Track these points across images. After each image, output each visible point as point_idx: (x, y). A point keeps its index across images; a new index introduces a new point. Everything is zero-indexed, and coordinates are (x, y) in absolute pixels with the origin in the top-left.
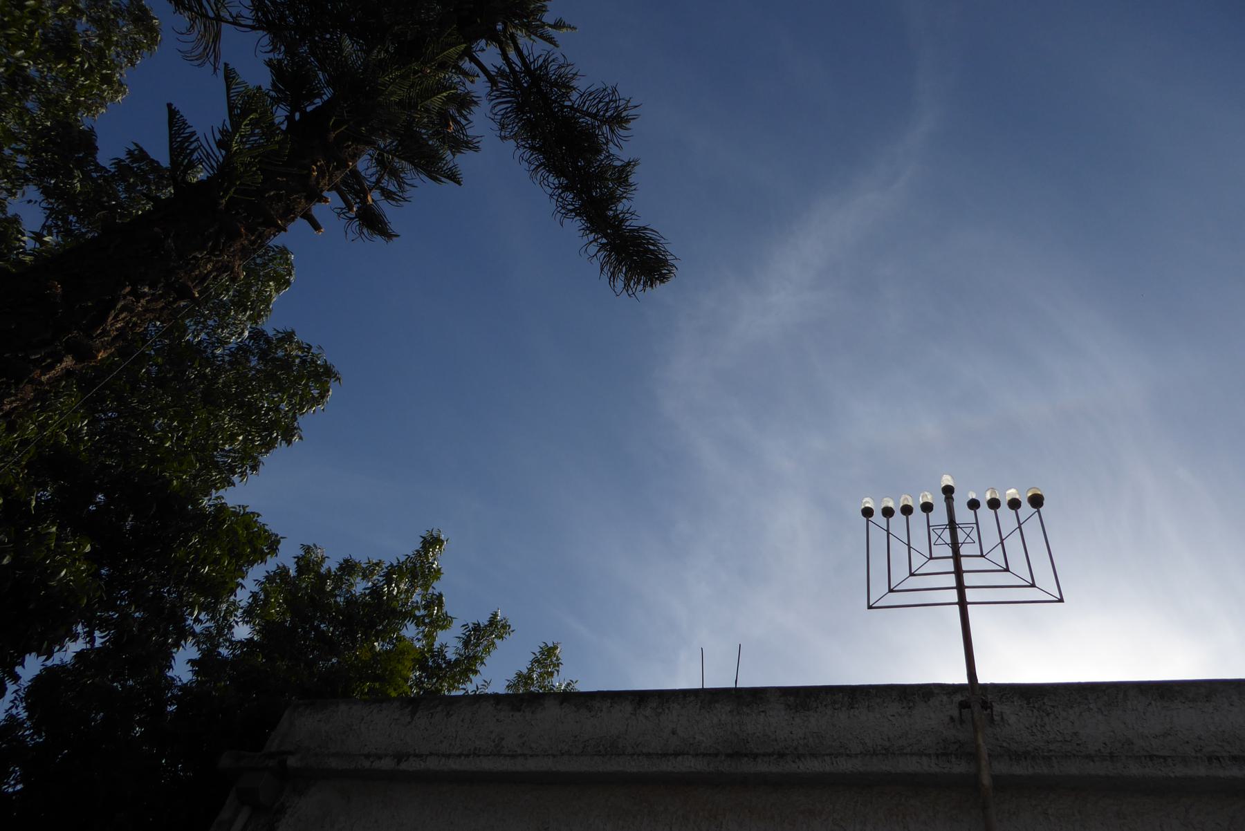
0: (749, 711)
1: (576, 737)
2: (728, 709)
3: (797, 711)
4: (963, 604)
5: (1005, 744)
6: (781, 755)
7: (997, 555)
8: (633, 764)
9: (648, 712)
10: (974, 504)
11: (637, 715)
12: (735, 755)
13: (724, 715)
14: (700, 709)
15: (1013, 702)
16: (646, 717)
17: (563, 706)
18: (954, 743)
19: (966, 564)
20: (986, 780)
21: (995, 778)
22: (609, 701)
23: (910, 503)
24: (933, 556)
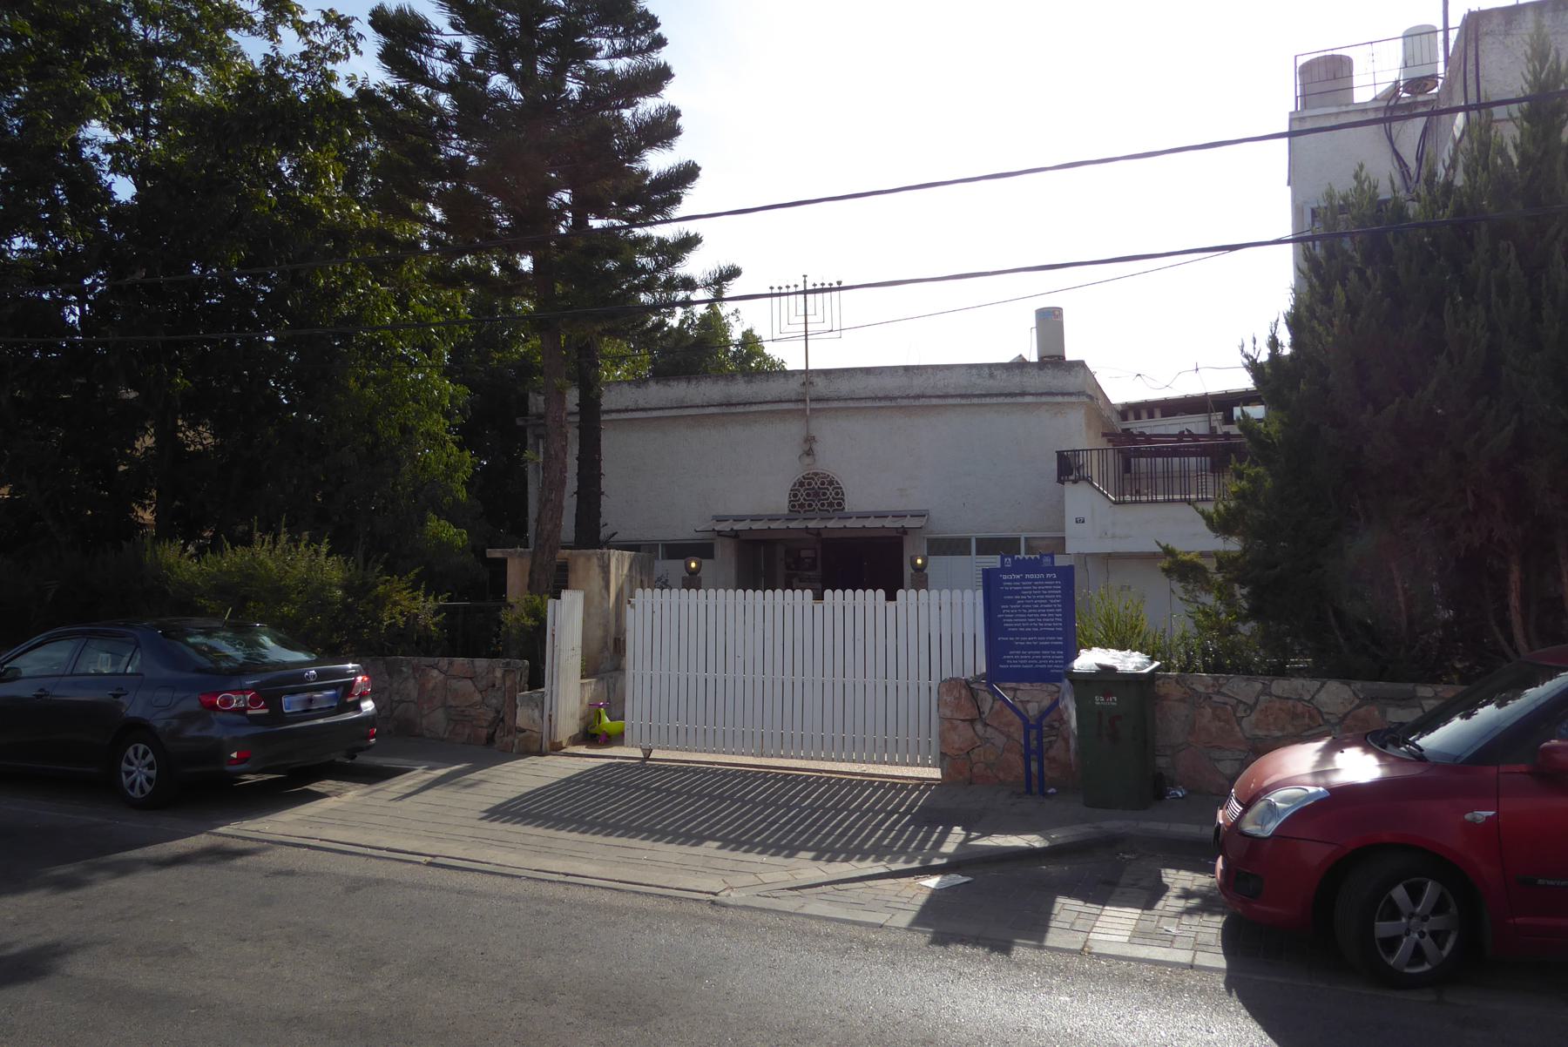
4: (806, 340)
21: (811, 409)
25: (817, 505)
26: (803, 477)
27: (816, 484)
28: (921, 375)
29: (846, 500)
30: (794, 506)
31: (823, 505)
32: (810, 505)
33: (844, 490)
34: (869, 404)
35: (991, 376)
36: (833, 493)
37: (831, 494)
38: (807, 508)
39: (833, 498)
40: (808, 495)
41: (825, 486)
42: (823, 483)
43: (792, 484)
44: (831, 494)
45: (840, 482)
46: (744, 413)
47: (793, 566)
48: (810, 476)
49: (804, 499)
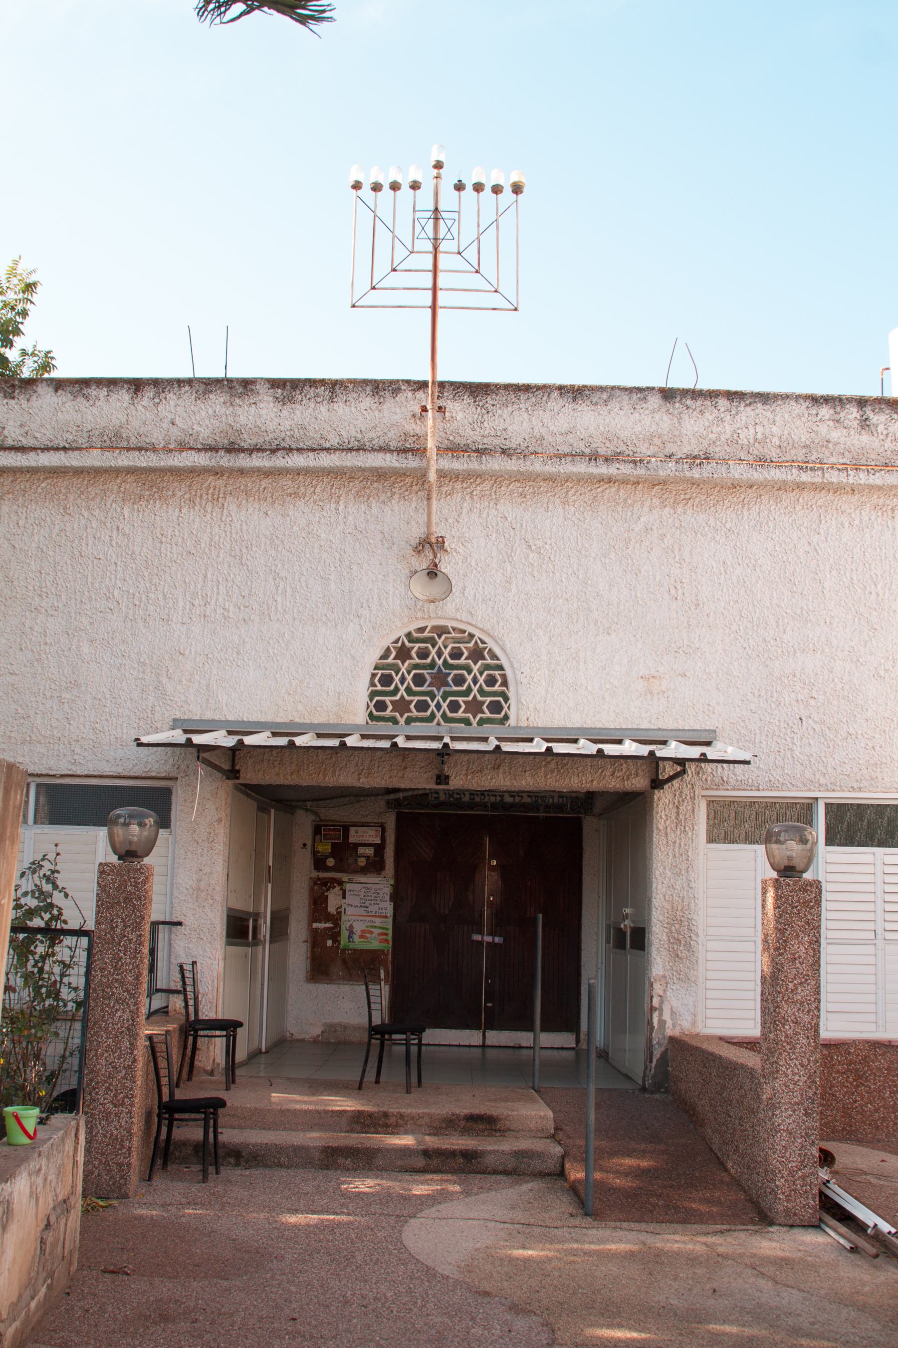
0: (241, 403)
1: (78, 426)
2: (222, 400)
3: (284, 404)
4: (434, 308)
5: (451, 438)
6: (274, 451)
7: (471, 254)
8: (142, 458)
9: (145, 402)
10: (459, 187)
11: (136, 405)
12: (232, 449)
13: (218, 407)
14: (196, 400)
15: (463, 400)
16: (144, 407)
17: (58, 394)
18: (413, 436)
19: (444, 262)
20: (432, 476)
22: (105, 389)
23: (400, 181)
24: (415, 250)
25: (438, 706)
26: (409, 635)
27: (438, 658)
28: (702, 412)
29: (511, 694)
30: (380, 706)
31: (454, 707)
32: (422, 706)
33: (509, 672)
34: (582, 468)
35: (865, 423)
36: (481, 680)
37: (475, 680)
38: (415, 713)
39: (481, 691)
40: (419, 680)
41: (462, 661)
42: (456, 654)
43: (379, 652)
44: (475, 680)
45: (497, 651)
46: (267, 473)
47: (331, 862)
48: (426, 634)
49: (408, 690)
